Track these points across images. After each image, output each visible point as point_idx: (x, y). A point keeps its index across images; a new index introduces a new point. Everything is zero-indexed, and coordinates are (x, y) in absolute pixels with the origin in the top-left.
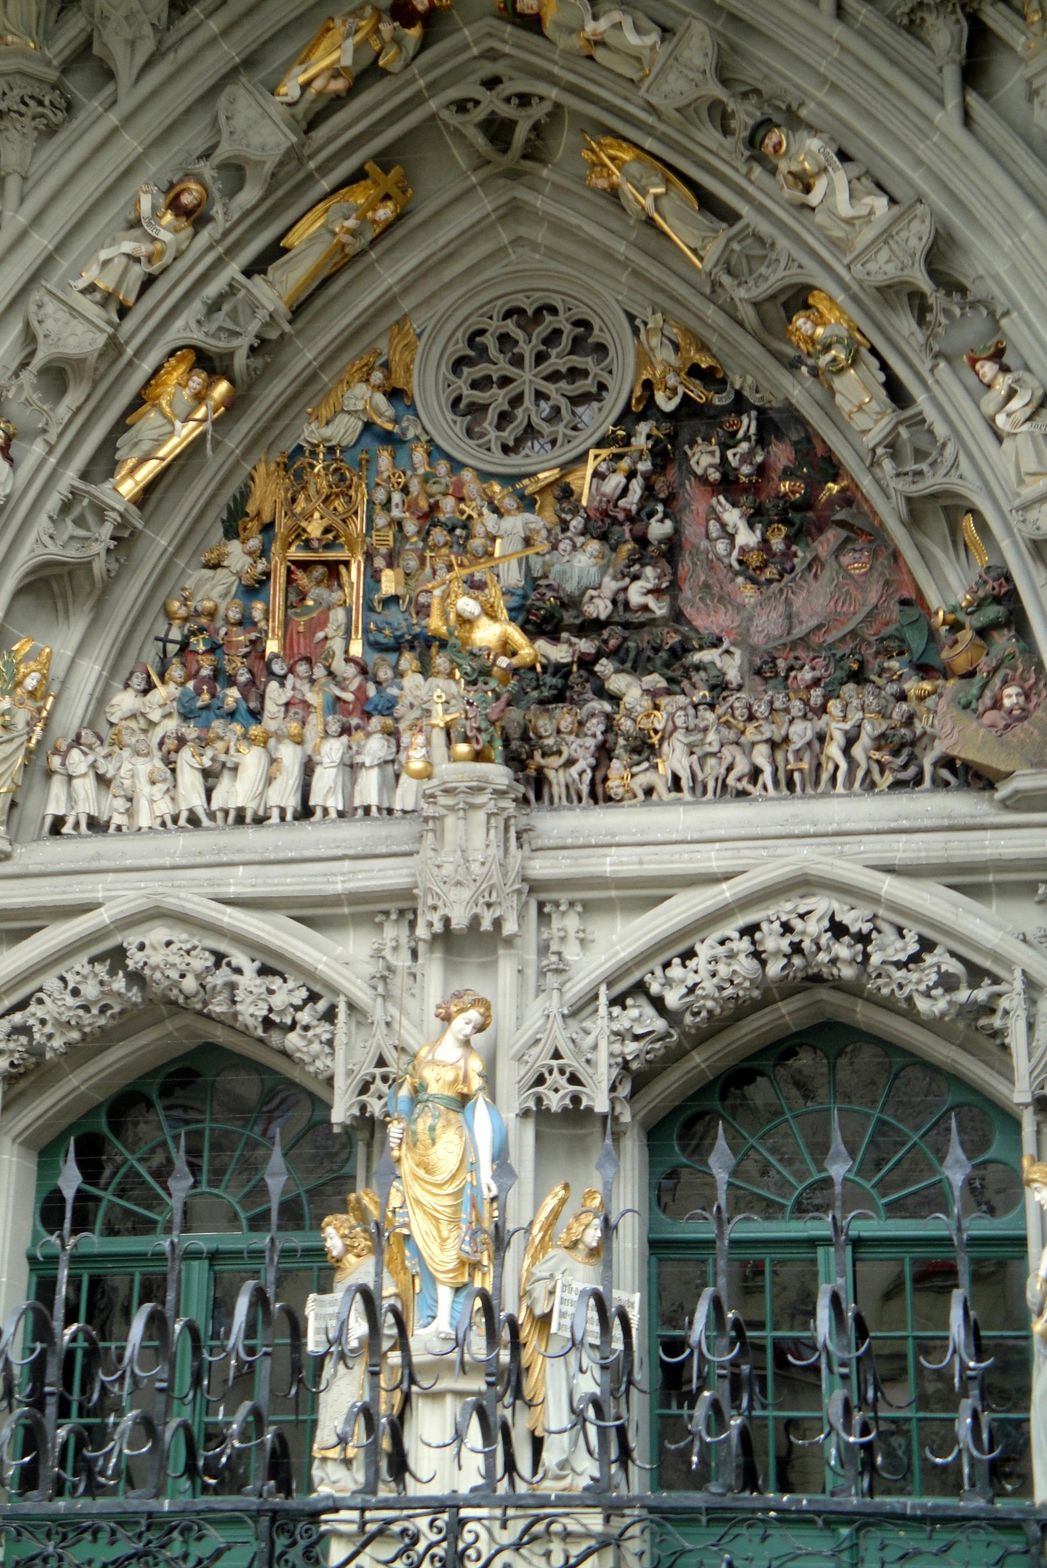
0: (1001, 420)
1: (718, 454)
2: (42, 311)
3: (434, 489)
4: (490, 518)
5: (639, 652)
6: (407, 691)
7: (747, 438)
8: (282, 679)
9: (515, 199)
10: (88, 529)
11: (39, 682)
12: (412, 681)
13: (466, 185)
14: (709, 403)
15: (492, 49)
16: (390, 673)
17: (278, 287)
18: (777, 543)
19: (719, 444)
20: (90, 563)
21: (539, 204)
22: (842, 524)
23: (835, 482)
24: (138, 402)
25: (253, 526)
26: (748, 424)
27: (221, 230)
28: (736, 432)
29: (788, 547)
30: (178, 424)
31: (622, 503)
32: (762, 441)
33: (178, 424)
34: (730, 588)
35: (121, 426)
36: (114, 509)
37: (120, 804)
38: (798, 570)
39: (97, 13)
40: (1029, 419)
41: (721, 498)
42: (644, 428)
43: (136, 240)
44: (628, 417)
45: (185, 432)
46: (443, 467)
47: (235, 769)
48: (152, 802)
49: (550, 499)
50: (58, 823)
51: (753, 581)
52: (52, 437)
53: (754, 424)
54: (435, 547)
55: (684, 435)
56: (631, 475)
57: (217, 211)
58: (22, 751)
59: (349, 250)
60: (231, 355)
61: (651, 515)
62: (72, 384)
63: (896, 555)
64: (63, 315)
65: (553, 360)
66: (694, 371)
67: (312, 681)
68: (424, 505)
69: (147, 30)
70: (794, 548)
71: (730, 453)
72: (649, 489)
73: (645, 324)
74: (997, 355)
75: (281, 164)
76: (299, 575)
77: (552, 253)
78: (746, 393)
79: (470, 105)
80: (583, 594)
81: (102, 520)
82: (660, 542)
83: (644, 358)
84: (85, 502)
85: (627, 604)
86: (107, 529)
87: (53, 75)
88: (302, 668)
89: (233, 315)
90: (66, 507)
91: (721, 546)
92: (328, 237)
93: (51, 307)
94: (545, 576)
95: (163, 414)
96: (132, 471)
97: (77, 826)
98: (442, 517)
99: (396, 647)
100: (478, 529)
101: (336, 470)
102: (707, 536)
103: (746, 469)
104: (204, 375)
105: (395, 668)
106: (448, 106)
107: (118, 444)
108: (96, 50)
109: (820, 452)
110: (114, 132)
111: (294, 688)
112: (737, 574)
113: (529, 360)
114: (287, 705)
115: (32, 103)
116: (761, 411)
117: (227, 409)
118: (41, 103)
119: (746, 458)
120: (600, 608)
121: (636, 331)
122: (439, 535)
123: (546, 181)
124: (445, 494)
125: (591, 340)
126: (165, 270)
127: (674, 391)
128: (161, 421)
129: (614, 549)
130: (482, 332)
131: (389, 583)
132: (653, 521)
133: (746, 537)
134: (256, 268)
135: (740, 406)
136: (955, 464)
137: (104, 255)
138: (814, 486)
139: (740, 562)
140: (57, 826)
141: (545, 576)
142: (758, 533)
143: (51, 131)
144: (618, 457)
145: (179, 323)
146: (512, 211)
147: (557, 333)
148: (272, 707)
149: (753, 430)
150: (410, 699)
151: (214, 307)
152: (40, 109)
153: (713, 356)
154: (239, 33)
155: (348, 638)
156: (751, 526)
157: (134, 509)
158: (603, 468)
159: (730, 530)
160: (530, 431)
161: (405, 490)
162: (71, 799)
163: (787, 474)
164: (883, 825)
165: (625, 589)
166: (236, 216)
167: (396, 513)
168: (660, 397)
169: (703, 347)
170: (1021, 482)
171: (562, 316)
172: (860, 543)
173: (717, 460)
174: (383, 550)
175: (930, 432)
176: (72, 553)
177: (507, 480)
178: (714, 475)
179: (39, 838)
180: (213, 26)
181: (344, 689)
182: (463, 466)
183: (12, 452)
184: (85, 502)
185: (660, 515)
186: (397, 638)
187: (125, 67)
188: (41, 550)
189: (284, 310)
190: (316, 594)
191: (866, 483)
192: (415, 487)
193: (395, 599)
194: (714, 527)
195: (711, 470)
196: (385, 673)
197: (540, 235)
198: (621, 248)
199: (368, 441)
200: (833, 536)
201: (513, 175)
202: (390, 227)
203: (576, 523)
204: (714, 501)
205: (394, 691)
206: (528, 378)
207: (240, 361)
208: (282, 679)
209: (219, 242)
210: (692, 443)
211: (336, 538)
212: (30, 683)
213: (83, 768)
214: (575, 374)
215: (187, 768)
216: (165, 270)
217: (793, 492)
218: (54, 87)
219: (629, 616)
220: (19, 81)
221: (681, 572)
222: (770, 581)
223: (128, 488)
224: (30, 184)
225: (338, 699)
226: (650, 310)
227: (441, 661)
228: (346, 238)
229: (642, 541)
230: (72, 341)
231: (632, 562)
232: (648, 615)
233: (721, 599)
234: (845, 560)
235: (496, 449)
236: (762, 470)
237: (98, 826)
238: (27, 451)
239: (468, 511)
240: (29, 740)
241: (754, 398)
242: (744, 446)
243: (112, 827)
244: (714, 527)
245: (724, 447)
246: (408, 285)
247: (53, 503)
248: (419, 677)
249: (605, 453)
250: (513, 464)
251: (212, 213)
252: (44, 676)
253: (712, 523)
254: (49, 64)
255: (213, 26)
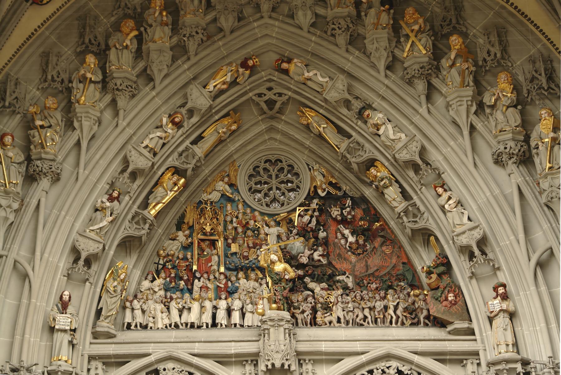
0: (447, 206)
1: (340, 211)
2: (131, 154)
3: (247, 217)
4: (266, 229)
5: (319, 275)
6: (241, 285)
7: (349, 207)
8: (199, 279)
9: (272, 125)
10: (140, 226)
11: (125, 276)
12: (243, 281)
13: (257, 120)
14: (336, 194)
15: (270, 79)
16: (235, 279)
17: (201, 149)
18: (361, 242)
19: (340, 208)
20: (141, 237)
21: (280, 127)
22: (382, 236)
23: (378, 222)
24: (156, 184)
25: (185, 226)
26: (349, 202)
27: (186, 130)
28: (346, 204)
29: (364, 243)
30: (169, 192)
31: (309, 225)
32: (353, 209)
33: (169, 192)
34: (346, 255)
35: (151, 192)
36: (149, 219)
37: (151, 319)
38: (369, 250)
39: (150, 60)
40: (455, 207)
41: (341, 225)
42: (315, 201)
43: (160, 132)
44: (309, 198)
45: (171, 195)
46: (248, 211)
47: (189, 309)
48: (162, 319)
49: (284, 222)
50: (129, 325)
51: (353, 253)
52: (131, 194)
53: (350, 202)
54: (249, 237)
55: (327, 204)
56: (312, 217)
57: (185, 124)
58: (120, 300)
59: (222, 139)
60: (186, 170)
61: (320, 230)
62: (138, 177)
63: (401, 247)
64: (137, 155)
65: (282, 177)
66: (331, 184)
67: (209, 280)
68: (244, 222)
69: (165, 67)
70: (366, 243)
71: (344, 211)
72: (318, 221)
73: (313, 168)
74: (442, 187)
75: (206, 110)
76: (202, 244)
77: (281, 142)
78: (347, 192)
79: (263, 95)
80: (298, 255)
81: (145, 223)
82: (322, 239)
83: (313, 179)
84: (140, 216)
85: (313, 259)
86: (147, 226)
87: (135, 79)
88: (205, 276)
89: (187, 157)
90: (133, 218)
91: (343, 242)
92: (217, 134)
93: (133, 152)
94: (285, 248)
95: (164, 188)
96: (154, 207)
97: (136, 326)
98: (250, 227)
99: (237, 269)
100: (262, 232)
101: (214, 209)
102: (336, 238)
103: (349, 217)
104: (178, 176)
105: (237, 276)
106: (255, 95)
107: (149, 198)
108: (148, 72)
109: (373, 212)
110: (154, 97)
111: (203, 282)
112: (348, 251)
113: (274, 177)
114: (201, 288)
115: (130, 87)
116: (352, 199)
117: (184, 188)
118: (132, 88)
119: (349, 213)
120: (304, 260)
121: (310, 169)
122: (249, 233)
123: (282, 120)
124: (250, 219)
125: (294, 172)
126: (168, 142)
127: (324, 190)
128: (163, 190)
129: (307, 241)
130: (258, 167)
131: (234, 248)
132: (320, 232)
133: (351, 239)
134: (194, 142)
135: (345, 195)
136: (428, 220)
137: (151, 136)
138: (372, 223)
139: (349, 246)
140: (129, 326)
141: (285, 248)
142: (355, 238)
143: (133, 96)
144: (306, 211)
145: (170, 159)
146: (271, 129)
147: (282, 169)
148: (196, 289)
149: (350, 204)
150: (242, 288)
151: (180, 155)
152: (132, 89)
153: (336, 179)
154: (192, 69)
155: (219, 266)
156: (352, 235)
157: (154, 219)
158: (302, 213)
159: (346, 237)
160: (275, 200)
161: (237, 217)
162: (133, 318)
163: (361, 219)
164: (367, 338)
165: (312, 254)
166: (190, 126)
167: (235, 225)
168: (320, 191)
169: (332, 177)
170: (455, 227)
171: (284, 163)
172: (388, 243)
173: (340, 213)
174: (231, 237)
175: (418, 209)
176: (137, 233)
177: (270, 215)
178: (339, 218)
179: (123, 330)
180: (186, 66)
181: (220, 283)
182: (255, 210)
183: (120, 199)
184: (140, 216)
185: (322, 230)
186: (236, 266)
187: (158, 78)
188: (126, 232)
189: (203, 156)
190: (207, 251)
191: (392, 224)
192: (240, 216)
193: (235, 253)
194: (339, 235)
195: (338, 216)
196: (233, 278)
197: (278, 137)
198: (308, 143)
199: (223, 201)
200: (379, 240)
201: (272, 118)
202: (234, 131)
203: (295, 231)
204: (339, 226)
205: (237, 285)
206: (274, 182)
207: (189, 172)
208: (199, 279)
209: (184, 134)
210: (331, 208)
211: (214, 232)
212: (122, 277)
213: (138, 307)
214: (288, 181)
215: (174, 308)
216: (168, 142)
217: (365, 225)
218: (135, 82)
219: (313, 263)
220: (125, 80)
221: (330, 250)
222: (359, 254)
223: (153, 212)
224: (126, 112)
225: (218, 286)
226: (314, 163)
227: (253, 275)
228: (223, 135)
229: (317, 238)
230: (140, 164)
231: (314, 245)
232: (320, 263)
233: (345, 259)
234: (384, 248)
235: (264, 204)
236: (354, 217)
237: (145, 327)
238: (123, 199)
239: (258, 225)
240: (121, 296)
241: (350, 194)
242: (348, 209)
243: (149, 328)
244: (339, 235)
245: (342, 209)
246: (237, 151)
247: (130, 216)
248: (245, 280)
249: (302, 209)
250: (270, 210)
251: (184, 124)
252: (126, 274)
253: (338, 234)
254: (133, 75)
255: (186, 66)
